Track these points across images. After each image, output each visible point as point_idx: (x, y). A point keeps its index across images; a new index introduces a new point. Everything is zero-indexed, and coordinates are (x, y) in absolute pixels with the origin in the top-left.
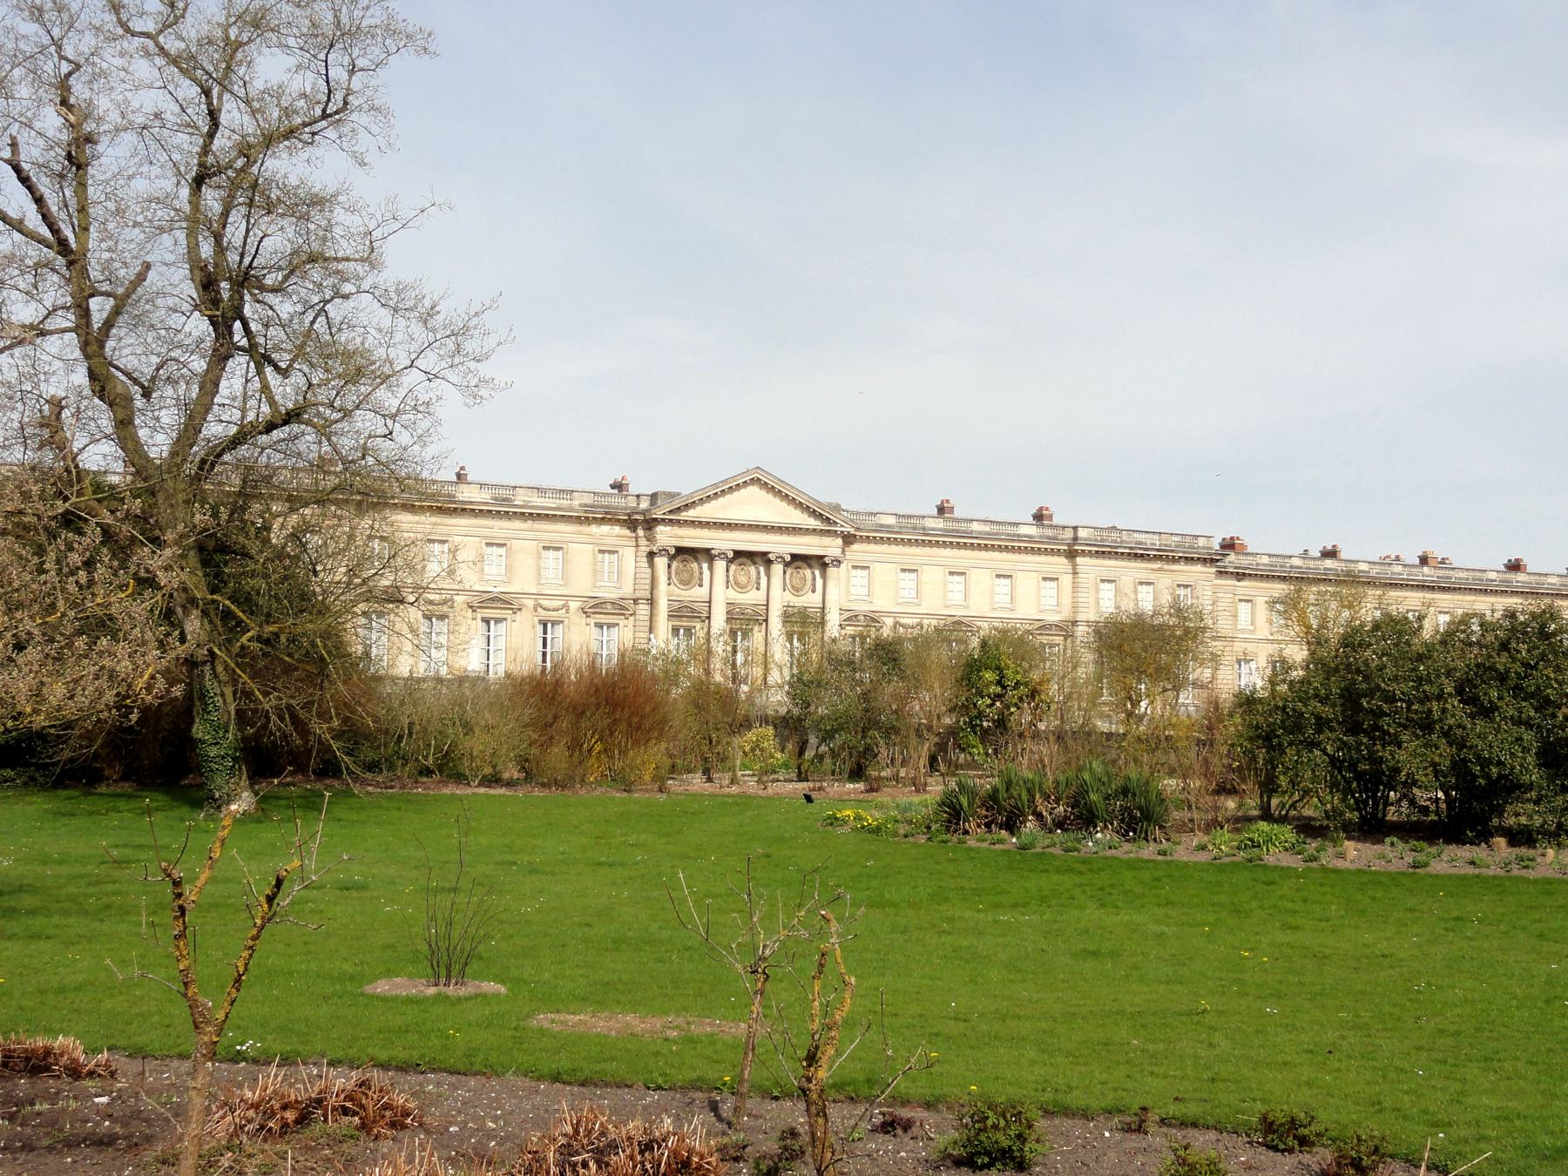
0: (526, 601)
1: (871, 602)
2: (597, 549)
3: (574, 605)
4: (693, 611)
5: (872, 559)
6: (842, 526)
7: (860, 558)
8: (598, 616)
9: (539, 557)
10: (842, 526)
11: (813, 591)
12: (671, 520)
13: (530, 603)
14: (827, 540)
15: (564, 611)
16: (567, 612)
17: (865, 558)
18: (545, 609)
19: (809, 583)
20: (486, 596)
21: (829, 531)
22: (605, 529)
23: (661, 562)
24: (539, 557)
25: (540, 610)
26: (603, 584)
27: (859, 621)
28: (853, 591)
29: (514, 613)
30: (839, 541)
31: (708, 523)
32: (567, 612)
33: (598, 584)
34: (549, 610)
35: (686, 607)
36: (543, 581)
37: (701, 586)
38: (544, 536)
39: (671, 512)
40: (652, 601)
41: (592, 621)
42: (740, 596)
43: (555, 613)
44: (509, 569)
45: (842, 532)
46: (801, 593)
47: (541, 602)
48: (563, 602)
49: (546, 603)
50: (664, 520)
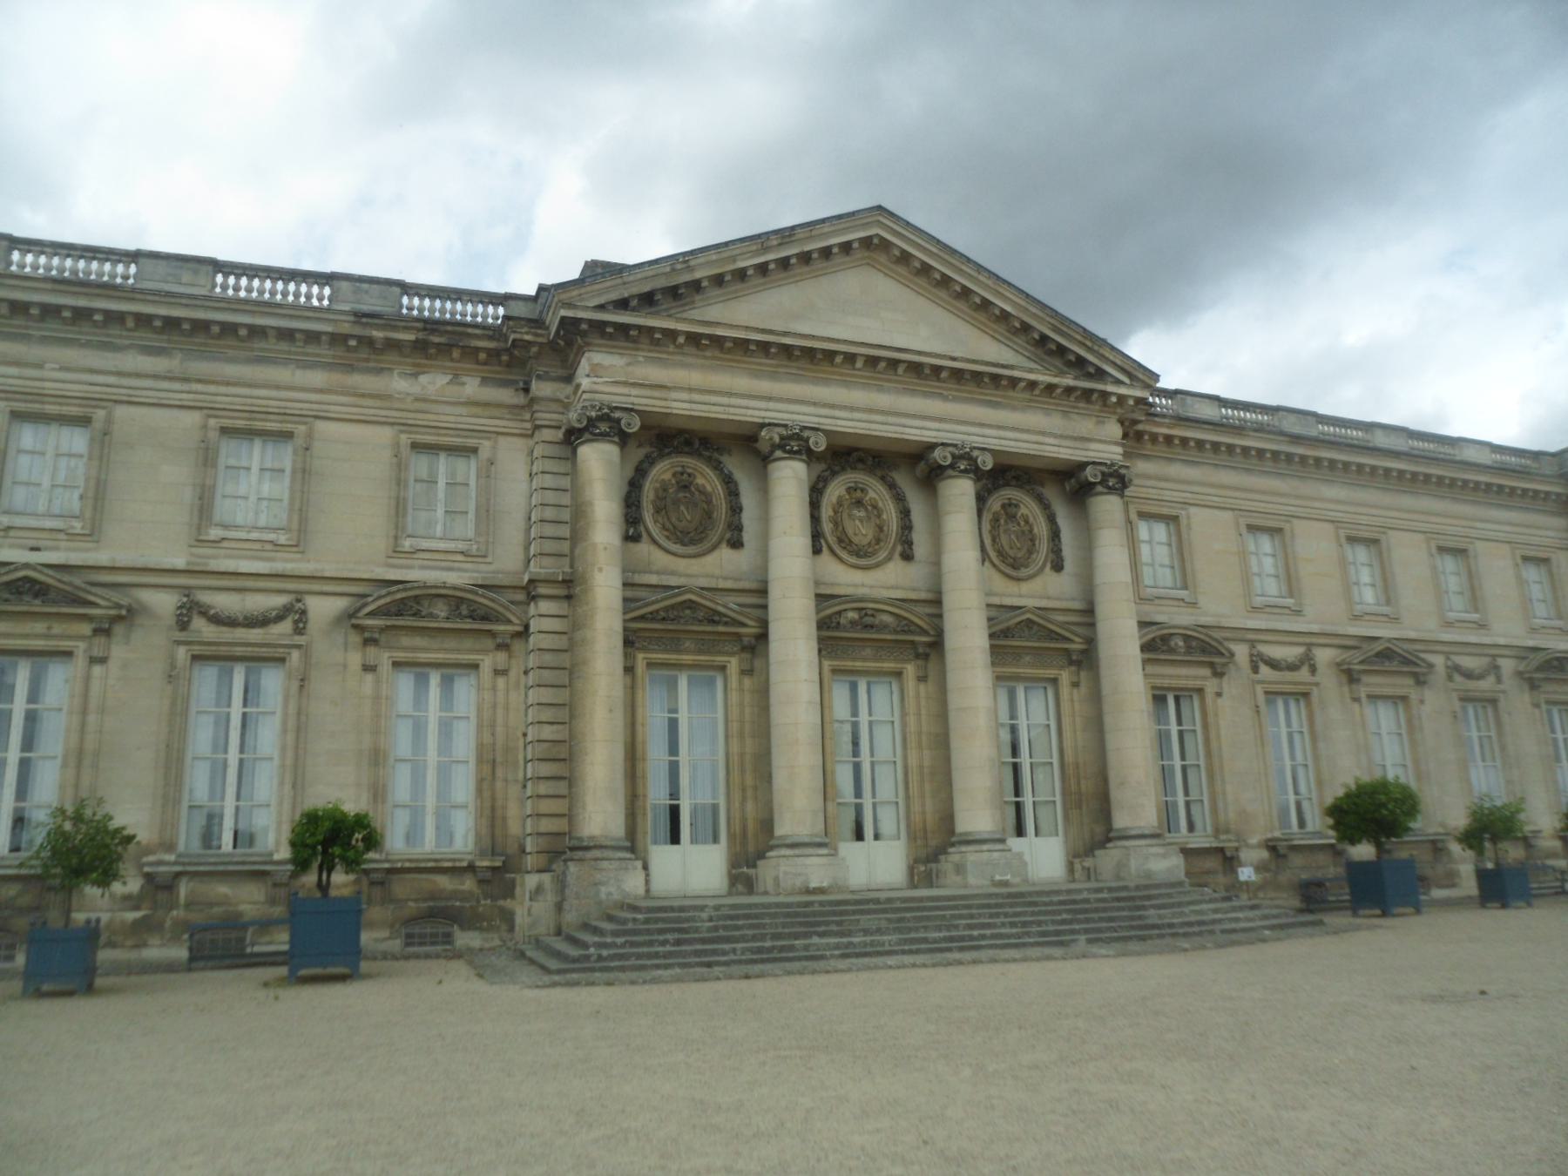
0: (149, 597)
1: (1194, 604)
2: (405, 439)
3: (323, 608)
4: (713, 617)
5: (1177, 496)
6: (1118, 382)
7: (1153, 493)
8: (406, 641)
9: (207, 458)
10: (1118, 382)
11: (1058, 567)
12: (623, 329)
13: (164, 603)
14: (1085, 426)
15: (286, 626)
16: (299, 631)
17: (1167, 495)
18: (218, 620)
19: (1044, 547)
21: (1087, 394)
22: (434, 382)
24: (207, 458)
25: (199, 623)
26: (425, 544)
27: (1172, 651)
29: (97, 631)
30: (1115, 430)
31: (742, 345)
32: (299, 631)
33: (407, 544)
34: (231, 622)
35: (691, 605)
36: (215, 533)
37: (737, 544)
38: (224, 396)
39: (622, 304)
40: (570, 588)
41: (384, 658)
42: (857, 577)
43: (255, 634)
44: (98, 496)
45: (1122, 399)
46: (1024, 572)
47: (206, 598)
48: (280, 601)
49: (225, 602)
50: (599, 327)
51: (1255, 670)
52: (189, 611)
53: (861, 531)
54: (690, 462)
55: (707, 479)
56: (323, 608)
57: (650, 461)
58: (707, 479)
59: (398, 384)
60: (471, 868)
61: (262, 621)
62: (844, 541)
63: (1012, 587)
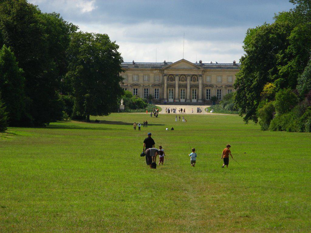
3: (150, 85)
19: (197, 80)
20: (134, 85)
22: (156, 71)
23: (165, 78)
28: (207, 80)
30: (201, 72)
42: (182, 83)
49: (145, 85)
51: (216, 87)
52: (143, 86)
53: (183, 80)
54: (172, 76)
55: (173, 77)
56: (150, 85)
57: (169, 76)
58: (173, 77)
59: (154, 72)
60: (159, 100)
61: (147, 86)
62: (182, 80)
63: (194, 83)
